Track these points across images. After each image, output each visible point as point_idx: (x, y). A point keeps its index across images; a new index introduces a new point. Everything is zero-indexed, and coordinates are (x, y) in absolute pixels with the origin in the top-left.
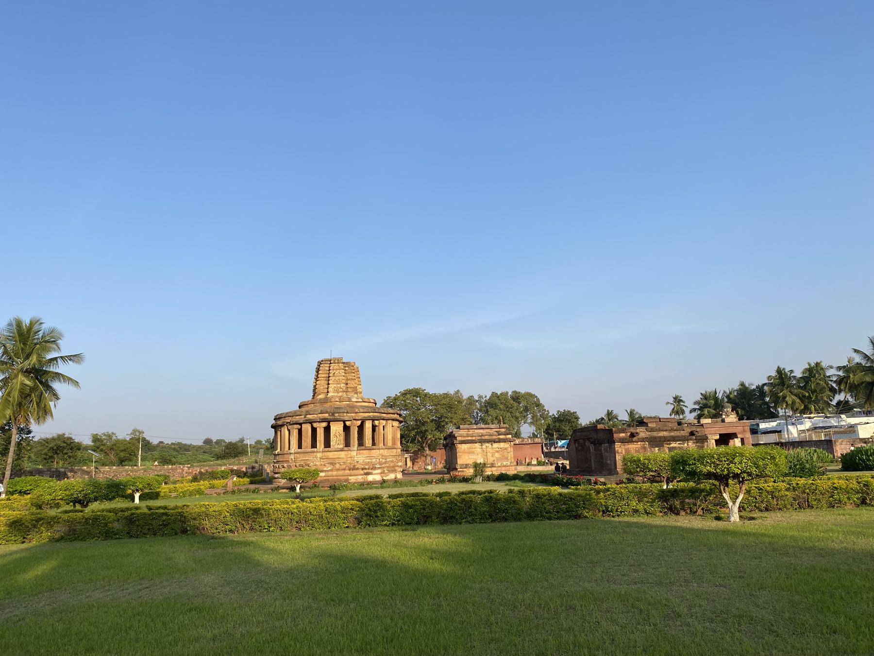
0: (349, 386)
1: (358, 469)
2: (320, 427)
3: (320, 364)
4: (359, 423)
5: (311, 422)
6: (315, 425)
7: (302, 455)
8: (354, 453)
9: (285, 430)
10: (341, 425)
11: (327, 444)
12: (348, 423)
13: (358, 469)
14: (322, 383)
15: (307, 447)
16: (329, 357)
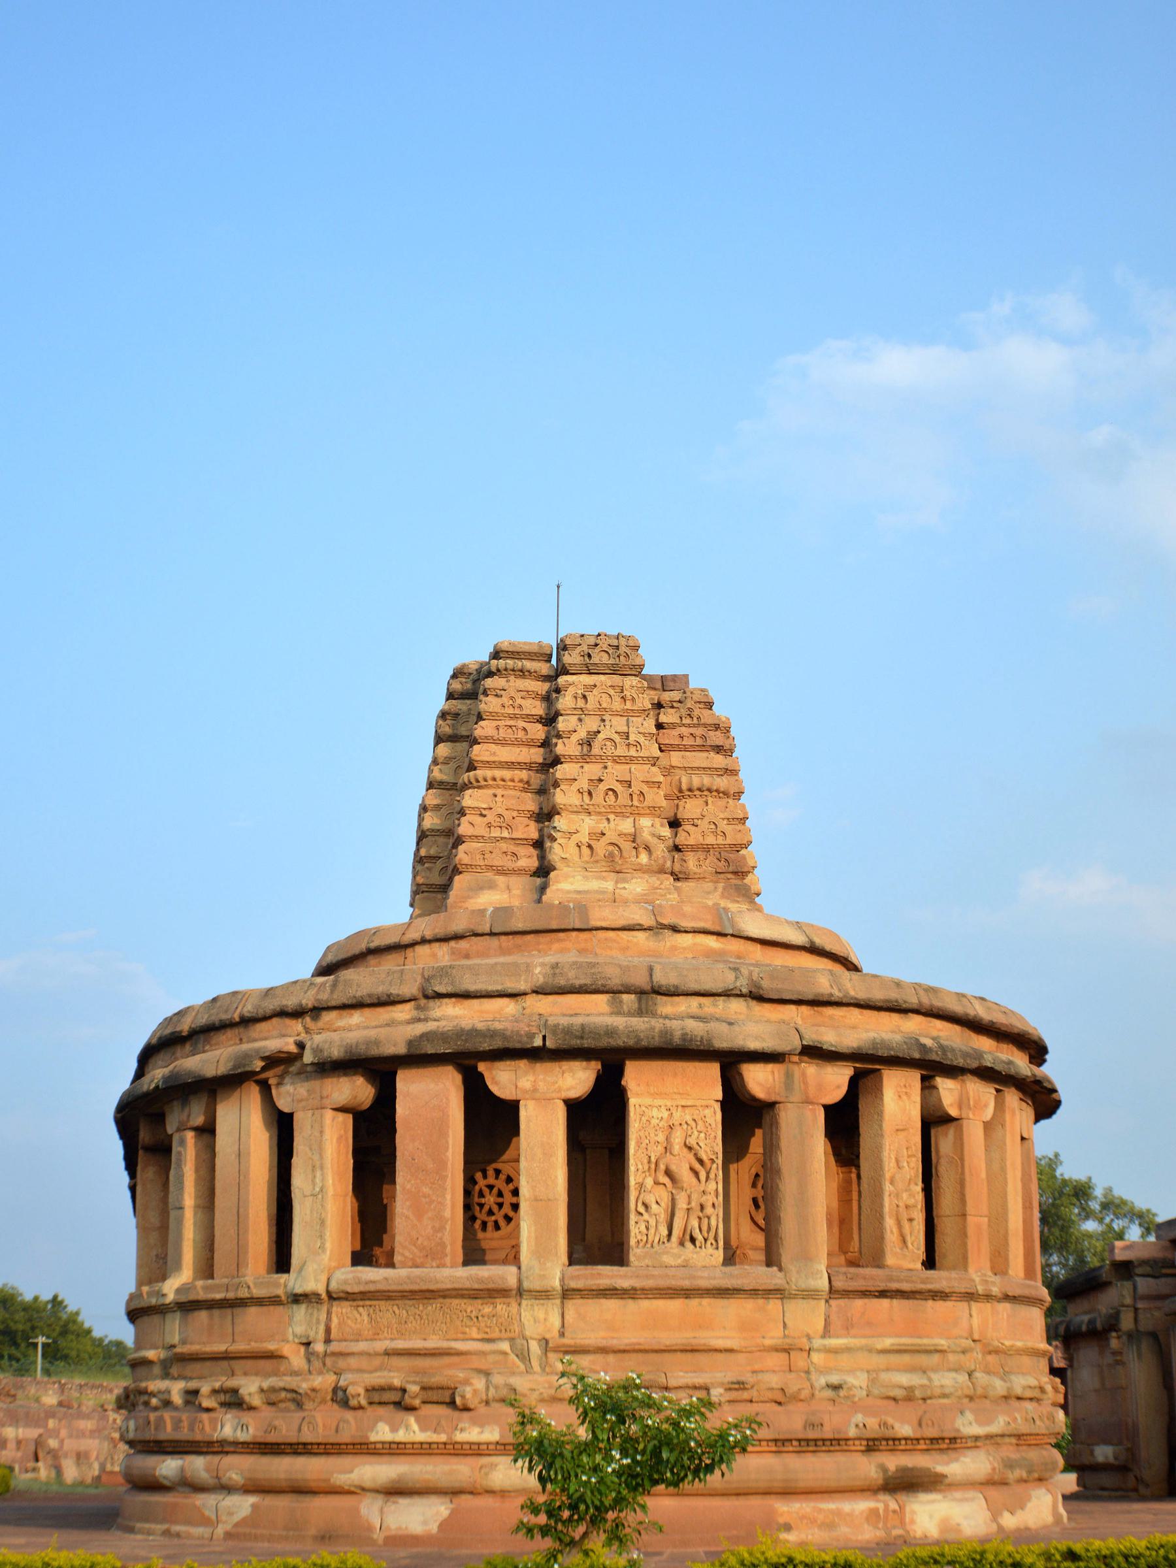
0: (689, 836)
1: (836, 1443)
2: (543, 1100)
3: (468, 687)
4: (835, 1081)
5: (467, 1060)
6: (503, 1080)
7: (388, 1313)
8: (807, 1318)
9: (243, 1126)
10: (705, 1085)
11: (598, 1230)
12: (759, 1080)
13: (836, 1443)
14: (494, 810)
15: (434, 1255)
16: (540, 633)
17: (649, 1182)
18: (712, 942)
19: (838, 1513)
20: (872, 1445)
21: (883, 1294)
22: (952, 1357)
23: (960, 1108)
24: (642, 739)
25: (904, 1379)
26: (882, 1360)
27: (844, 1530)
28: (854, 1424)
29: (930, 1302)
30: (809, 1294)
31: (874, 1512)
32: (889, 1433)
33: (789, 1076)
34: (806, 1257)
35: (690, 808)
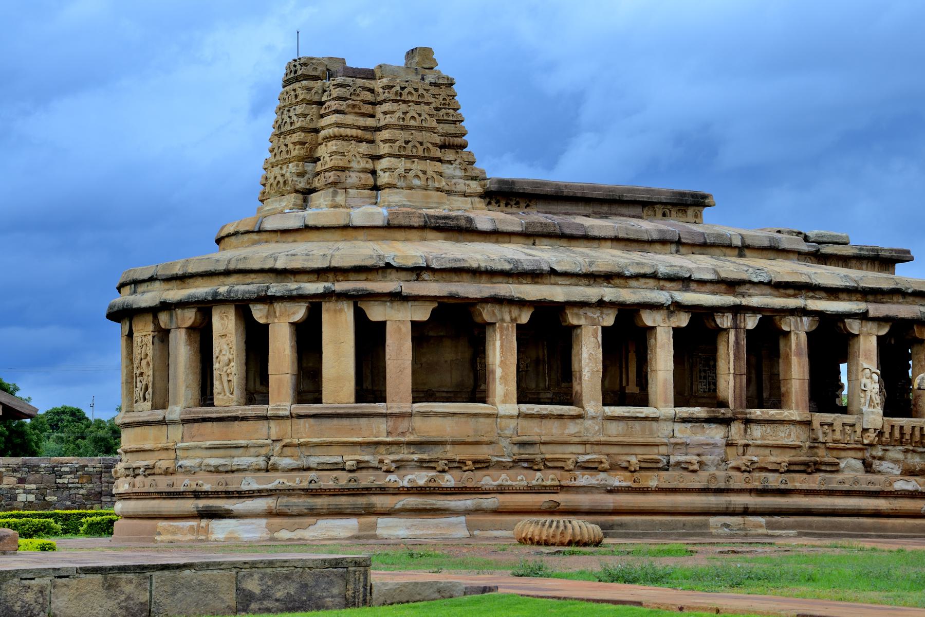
8: (176, 433)
17: (138, 372)
18: (255, 237)
19: (177, 527)
20: (197, 495)
21: (204, 420)
22: (252, 450)
23: (267, 317)
24: (294, 118)
25: (214, 462)
26: (208, 453)
27: (179, 537)
28: (182, 483)
29: (237, 422)
30: (173, 422)
31: (192, 527)
32: (198, 489)
33: (171, 316)
34: (175, 403)
35: (322, 152)
